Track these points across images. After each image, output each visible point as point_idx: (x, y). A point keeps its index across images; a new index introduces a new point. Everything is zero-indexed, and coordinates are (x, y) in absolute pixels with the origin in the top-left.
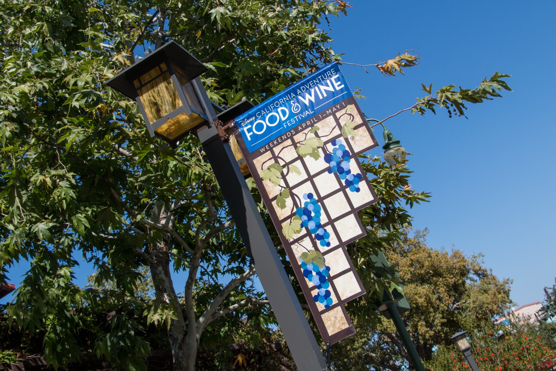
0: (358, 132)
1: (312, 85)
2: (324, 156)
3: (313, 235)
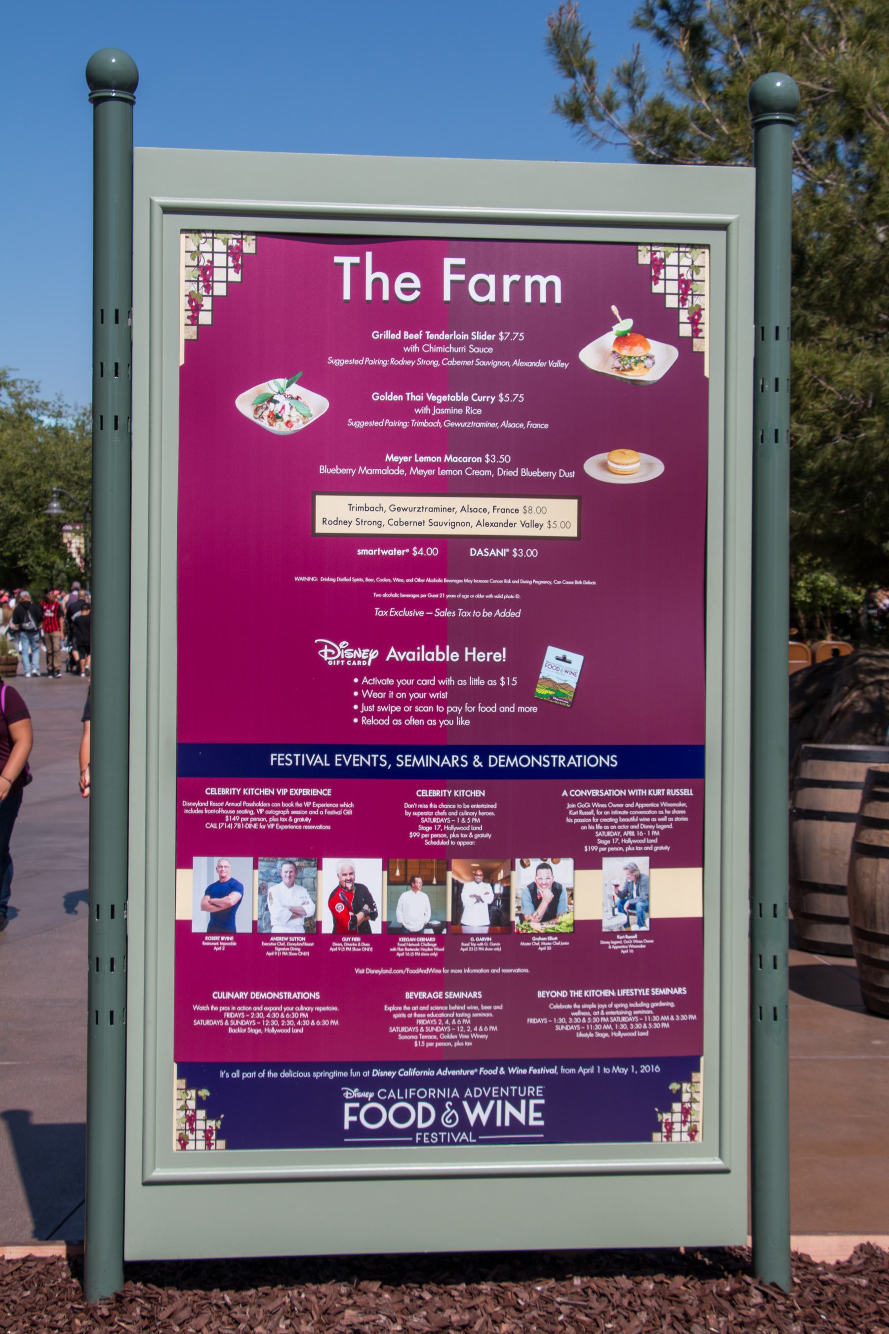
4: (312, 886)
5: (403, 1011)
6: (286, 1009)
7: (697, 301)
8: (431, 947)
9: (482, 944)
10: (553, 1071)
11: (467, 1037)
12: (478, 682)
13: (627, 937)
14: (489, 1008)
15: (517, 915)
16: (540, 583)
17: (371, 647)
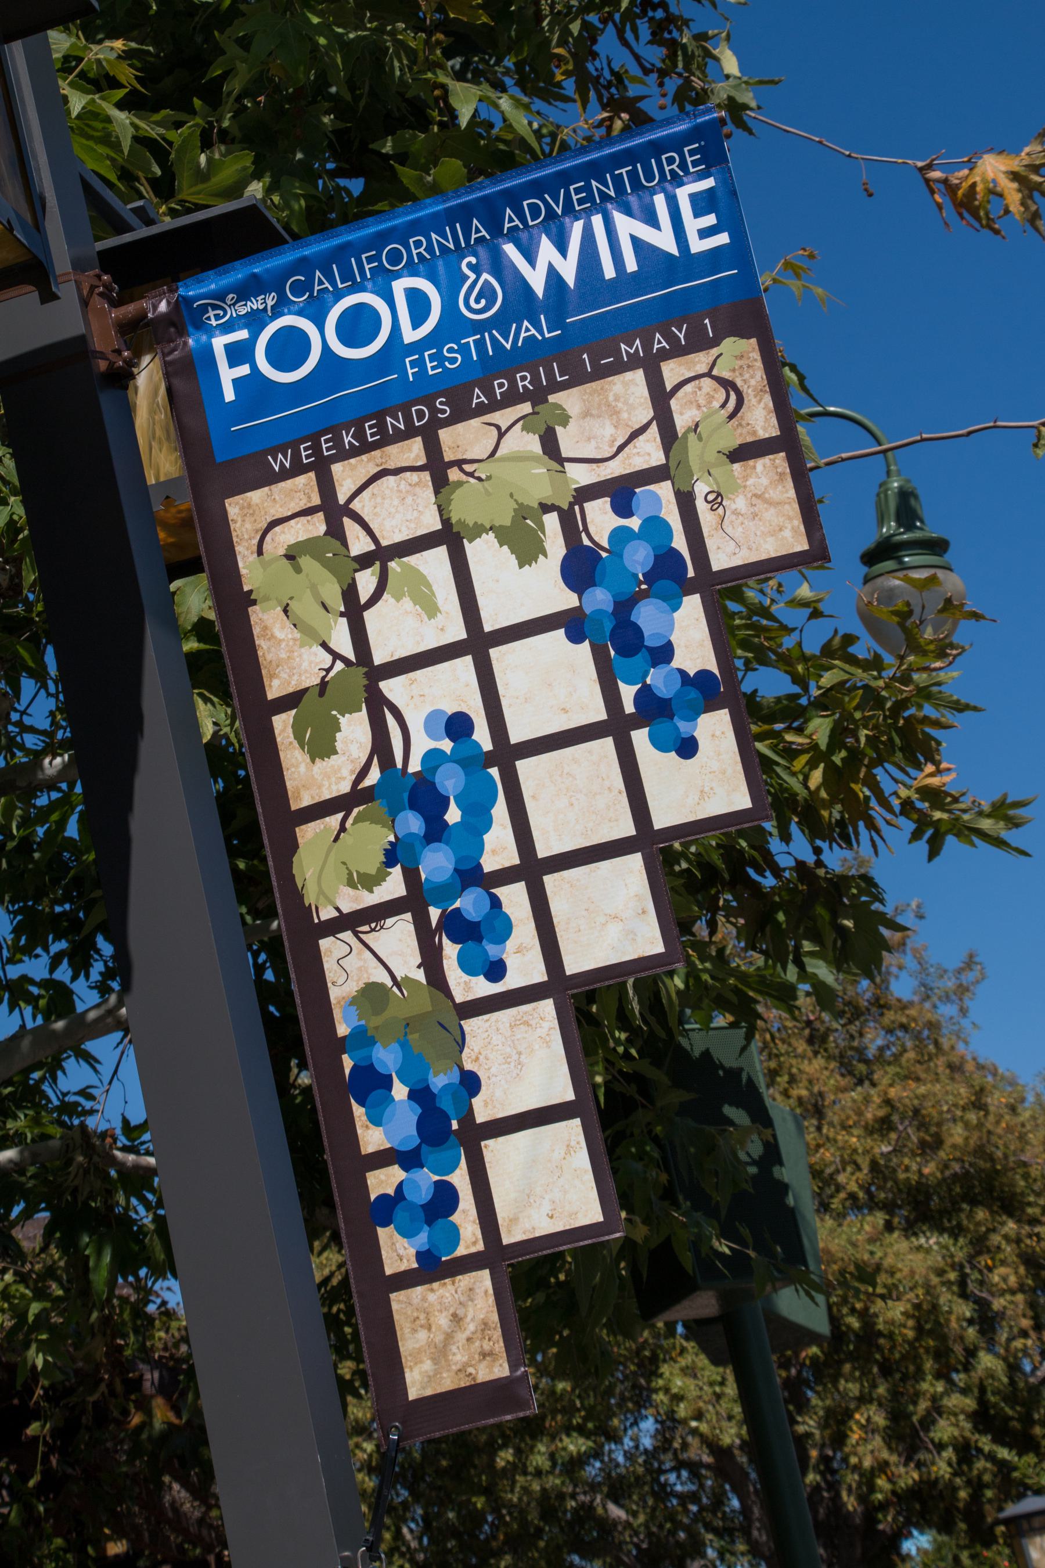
0: (746, 478)
1: (580, 202)
2: (563, 551)
3: (434, 914)
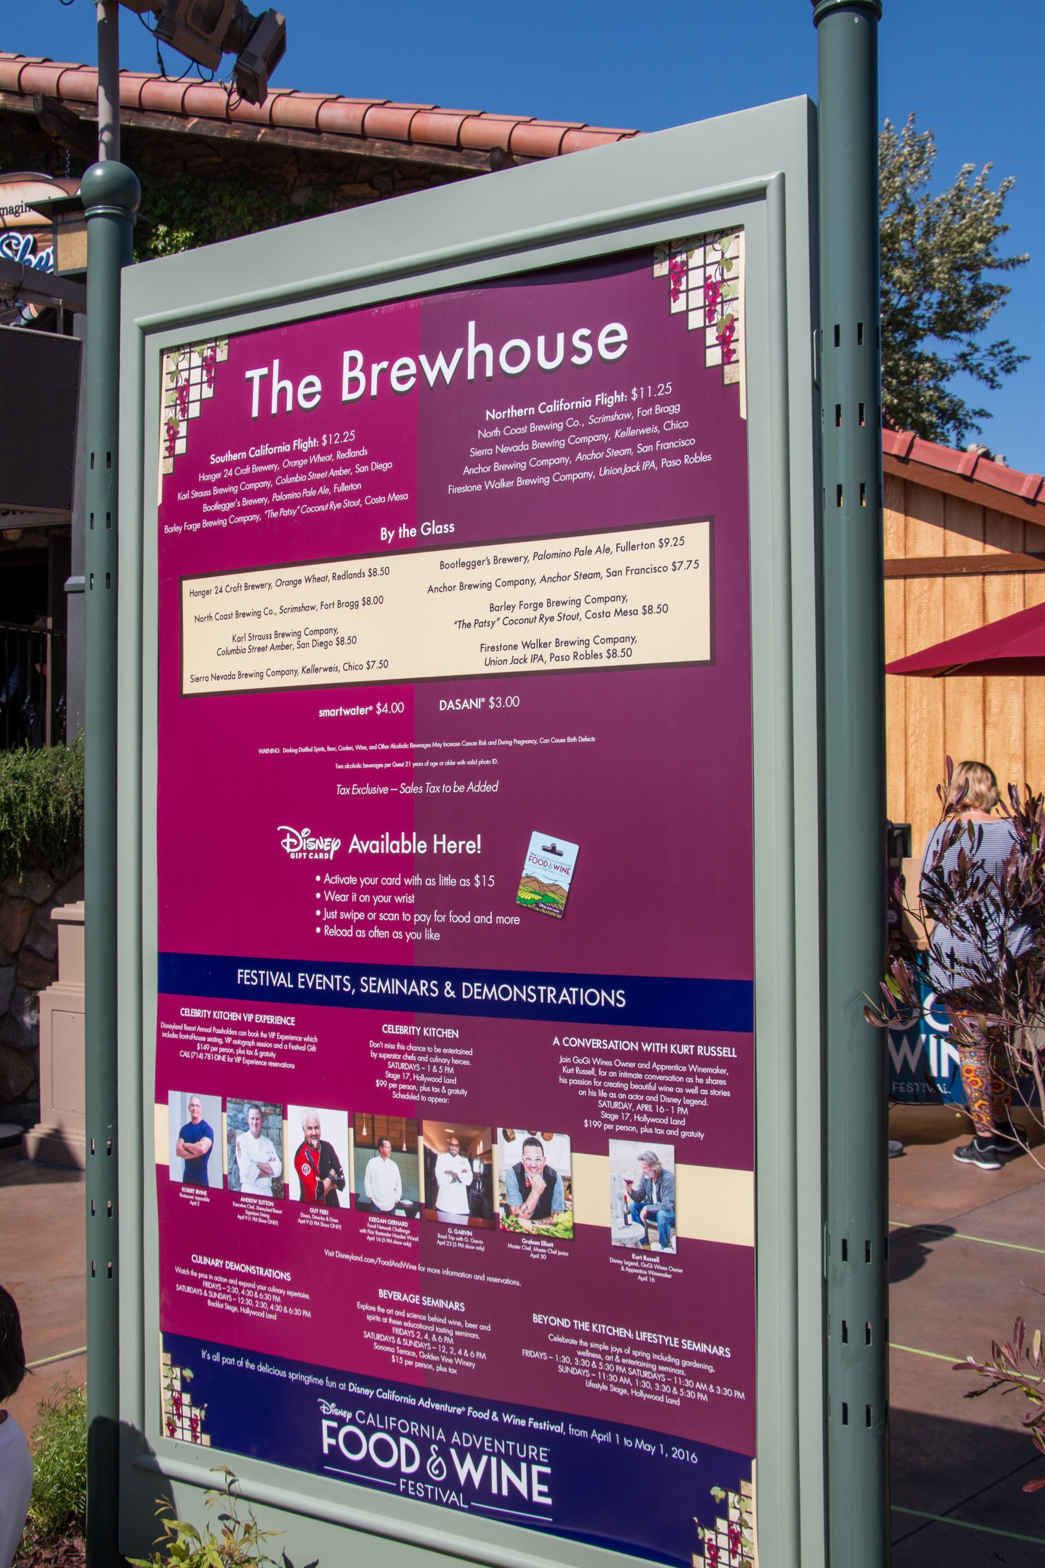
1: (488, 1447)
4: (278, 1139)
5: (376, 1313)
6: (259, 1287)
7: (729, 309)
8: (404, 1234)
9: (461, 1239)
10: (559, 1429)
11: (451, 1361)
12: (448, 881)
13: (645, 1257)
14: (474, 1326)
15: (501, 1205)
16: (521, 743)
17: (333, 835)
